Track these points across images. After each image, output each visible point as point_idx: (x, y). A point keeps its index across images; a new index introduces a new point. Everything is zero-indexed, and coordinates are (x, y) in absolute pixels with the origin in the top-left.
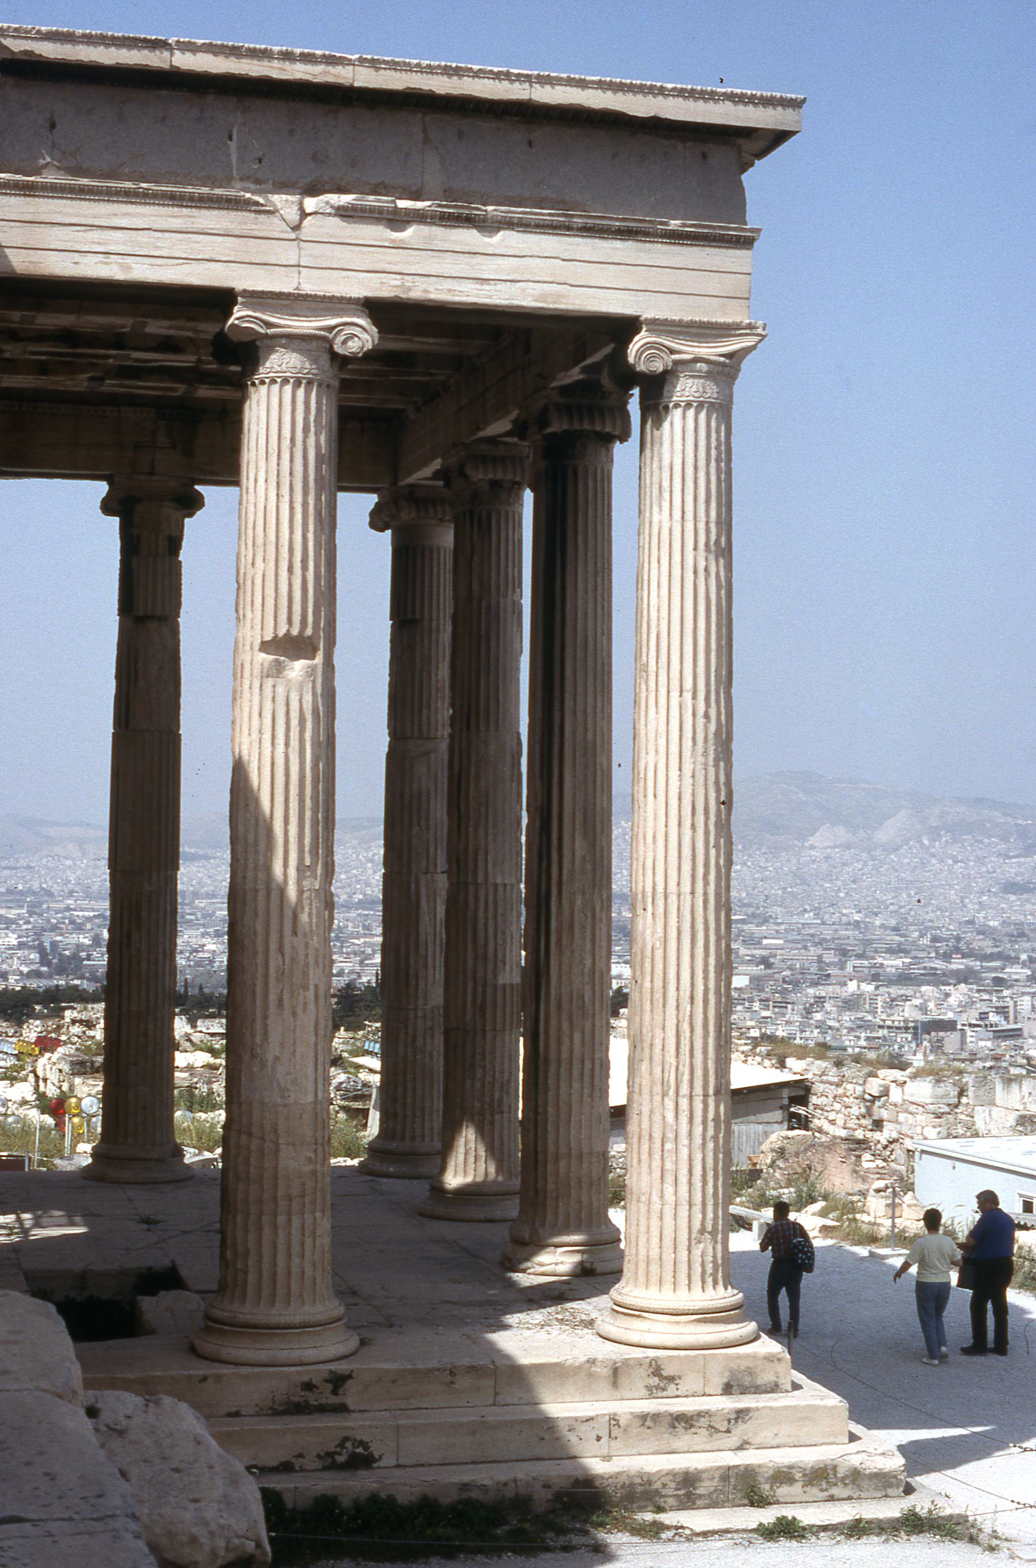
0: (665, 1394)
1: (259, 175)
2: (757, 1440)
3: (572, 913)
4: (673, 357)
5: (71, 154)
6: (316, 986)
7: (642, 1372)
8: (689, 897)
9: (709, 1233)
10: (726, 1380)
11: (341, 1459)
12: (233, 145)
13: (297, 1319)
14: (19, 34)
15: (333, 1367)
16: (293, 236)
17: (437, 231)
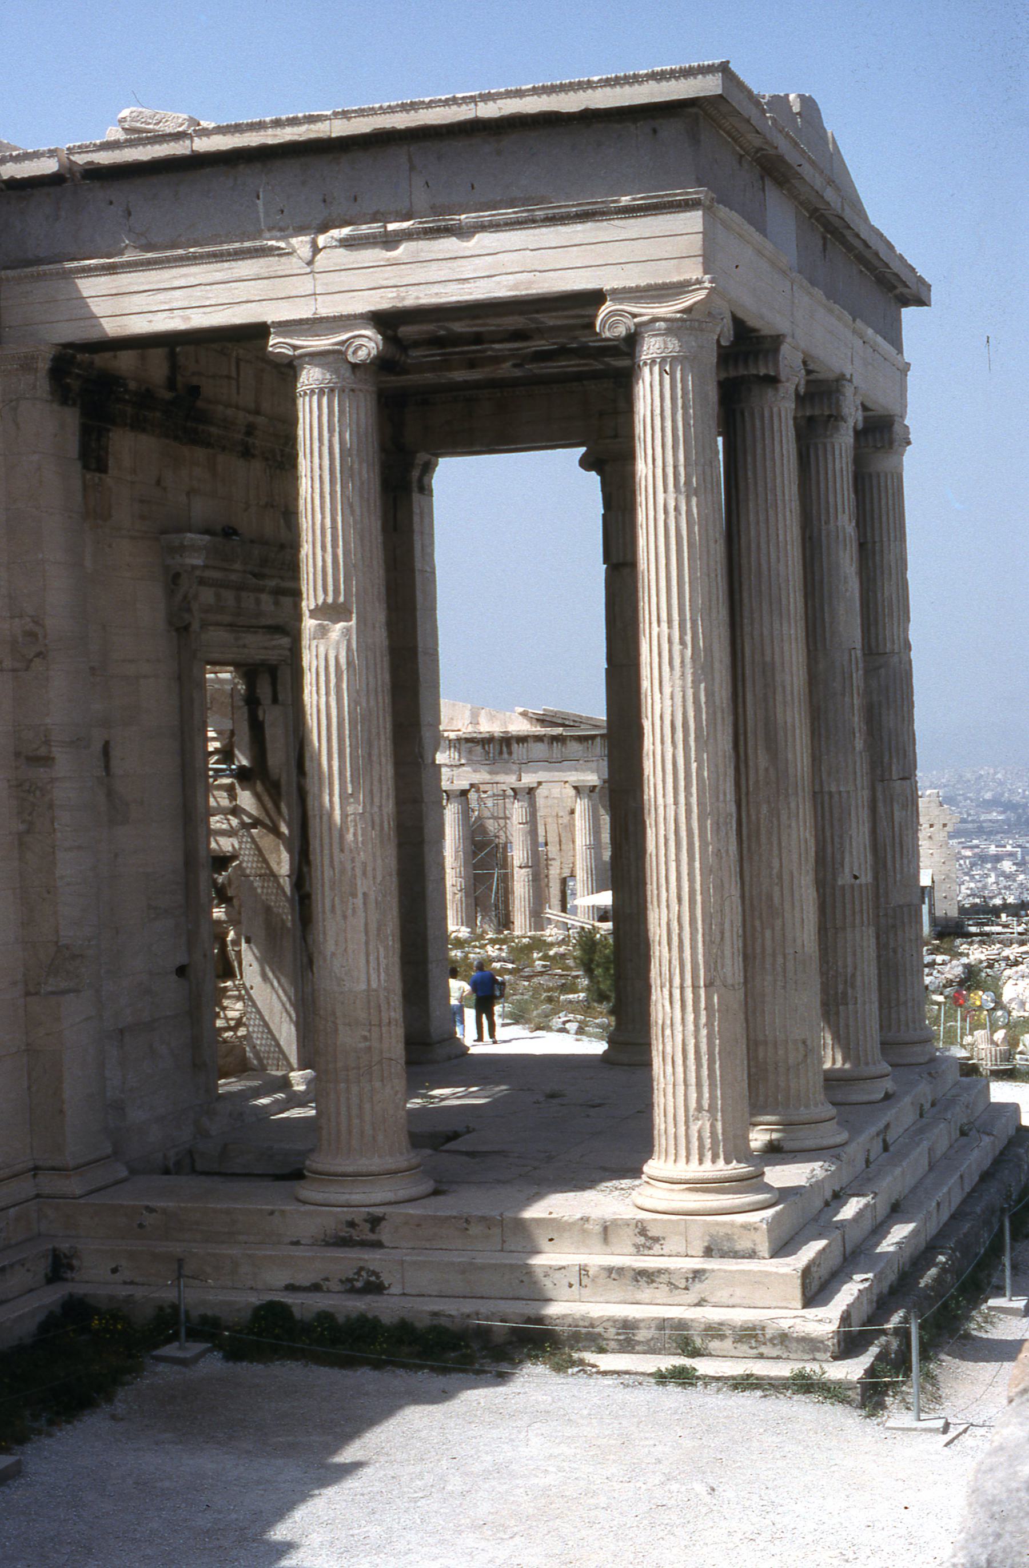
0: (651, 1252)
1: (281, 224)
2: (713, 1300)
3: (758, 819)
4: (636, 320)
5: (142, 235)
6: (364, 894)
7: (630, 1231)
8: (673, 807)
9: (707, 1111)
10: (706, 1244)
11: (359, 1285)
12: (260, 202)
13: (350, 1169)
14: (83, 149)
15: (371, 1210)
16: (308, 270)
17: (422, 244)
